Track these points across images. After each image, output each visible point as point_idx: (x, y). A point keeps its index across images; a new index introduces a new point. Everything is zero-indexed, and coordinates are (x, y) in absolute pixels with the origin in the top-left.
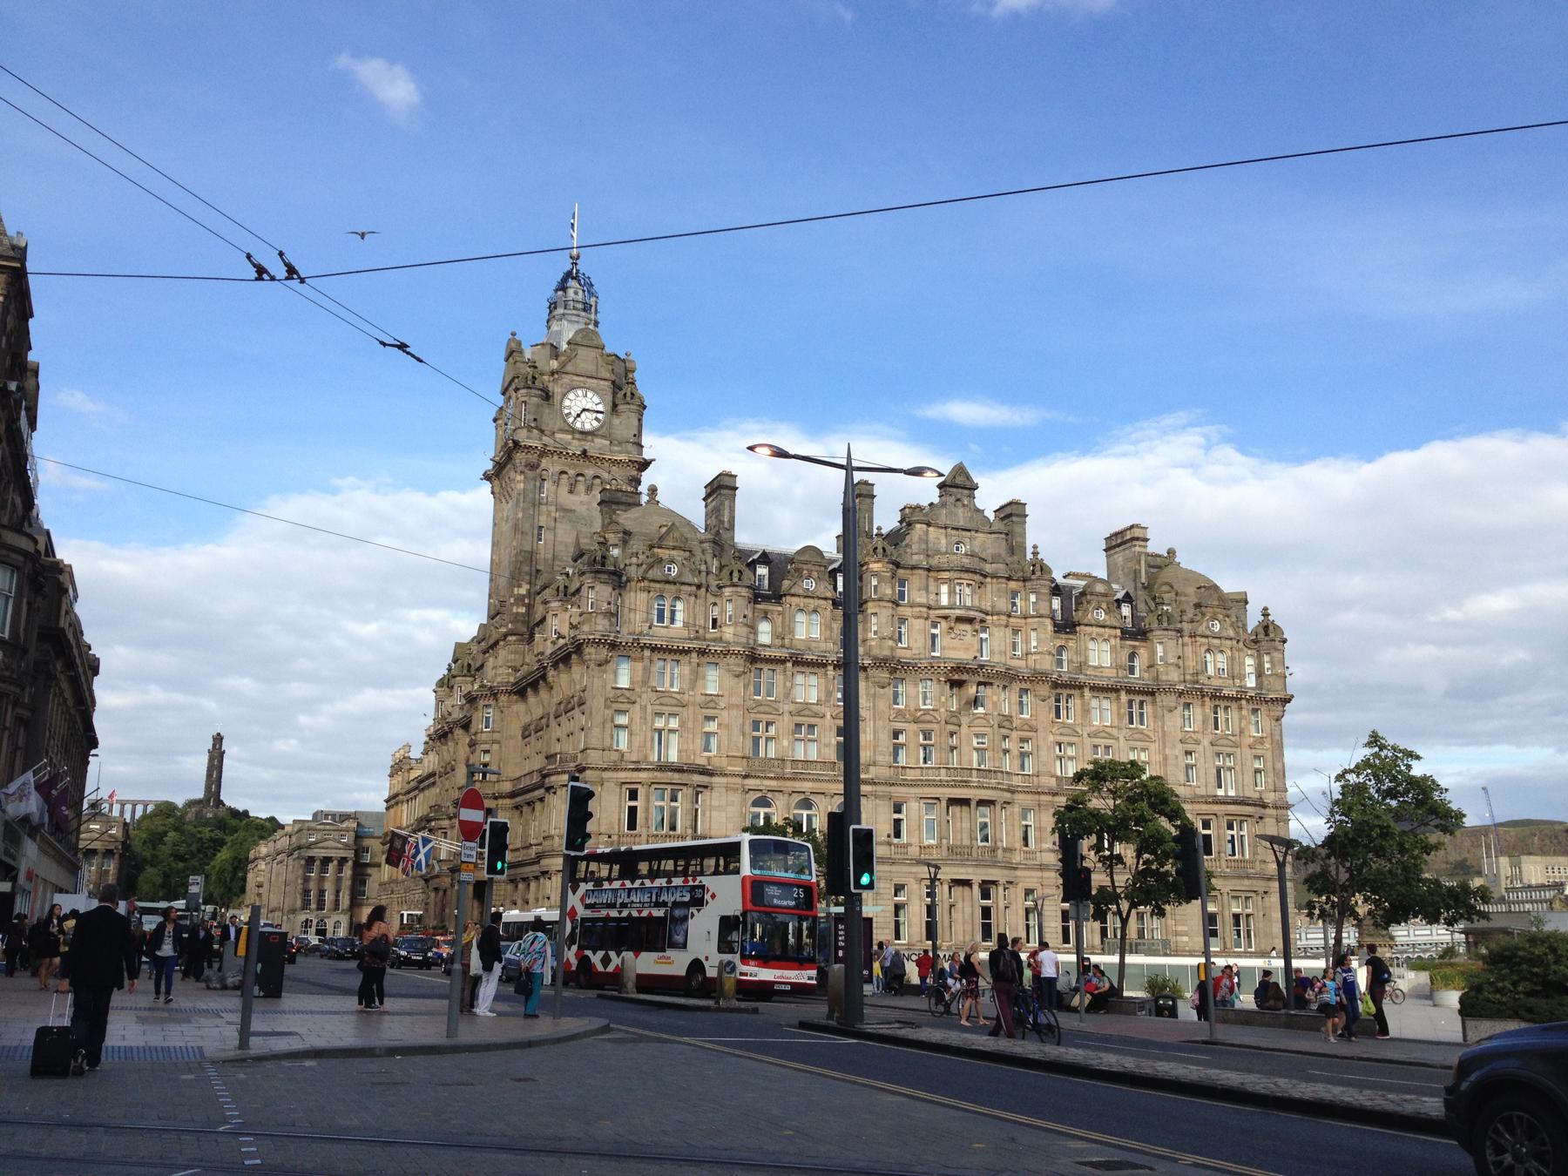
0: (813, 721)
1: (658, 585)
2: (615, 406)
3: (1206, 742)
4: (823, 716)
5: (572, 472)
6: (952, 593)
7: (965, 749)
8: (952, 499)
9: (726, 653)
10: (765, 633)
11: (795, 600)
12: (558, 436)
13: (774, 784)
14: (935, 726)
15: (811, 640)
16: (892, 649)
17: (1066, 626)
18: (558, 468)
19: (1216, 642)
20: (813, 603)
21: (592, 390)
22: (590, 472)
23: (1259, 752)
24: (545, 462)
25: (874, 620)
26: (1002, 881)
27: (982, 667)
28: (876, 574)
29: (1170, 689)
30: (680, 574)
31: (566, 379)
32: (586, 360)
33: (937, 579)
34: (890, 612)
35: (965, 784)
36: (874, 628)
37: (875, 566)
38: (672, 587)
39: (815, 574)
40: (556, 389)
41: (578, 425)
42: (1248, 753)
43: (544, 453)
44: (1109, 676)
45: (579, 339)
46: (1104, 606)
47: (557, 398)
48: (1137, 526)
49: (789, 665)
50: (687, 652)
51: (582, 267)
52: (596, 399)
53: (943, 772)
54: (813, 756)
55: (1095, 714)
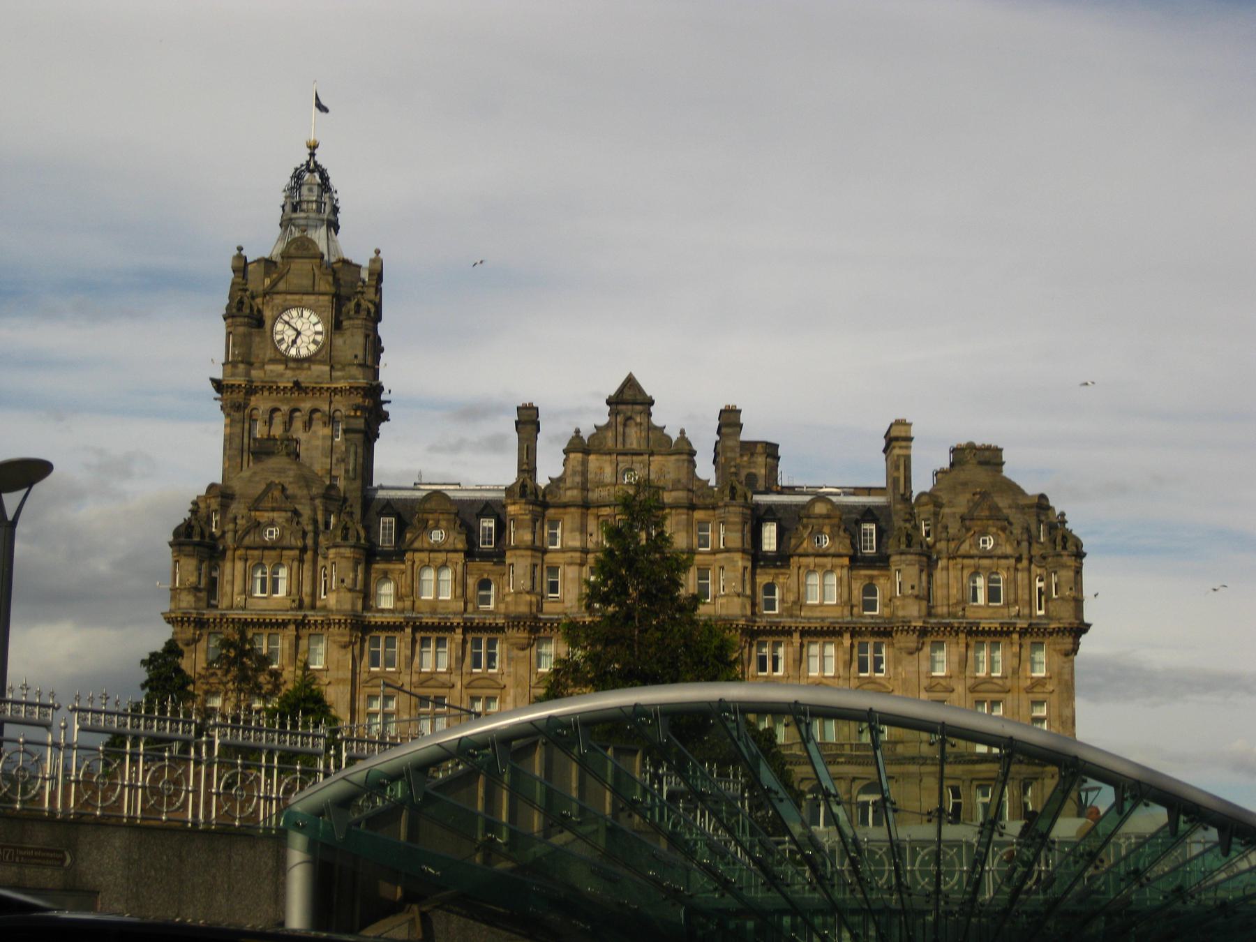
0: (440, 692)
1: (256, 553)
2: (336, 326)
3: (960, 689)
4: (453, 686)
5: (285, 408)
8: (620, 419)
9: (328, 624)
10: (386, 596)
11: (418, 556)
12: (269, 367)
18: (270, 405)
19: (985, 562)
20: (441, 557)
21: (310, 308)
22: (306, 406)
23: (1040, 697)
24: (254, 401)
29: (907, 629)
30: (282, 537)
31: (278, 299)
32: (300, 270)
34: (528, 561)
38: (273, 553)
39: (443, 523)
40: (268, 313)
41: (293, 352)
42: (1025, 699)
43: (251, 390)
45: (292, 251)
46: (827, 529)
47: (268, 323)
50: (284, 624)
51: (320, 158)
52: (314, 319)
55: (815, 664)
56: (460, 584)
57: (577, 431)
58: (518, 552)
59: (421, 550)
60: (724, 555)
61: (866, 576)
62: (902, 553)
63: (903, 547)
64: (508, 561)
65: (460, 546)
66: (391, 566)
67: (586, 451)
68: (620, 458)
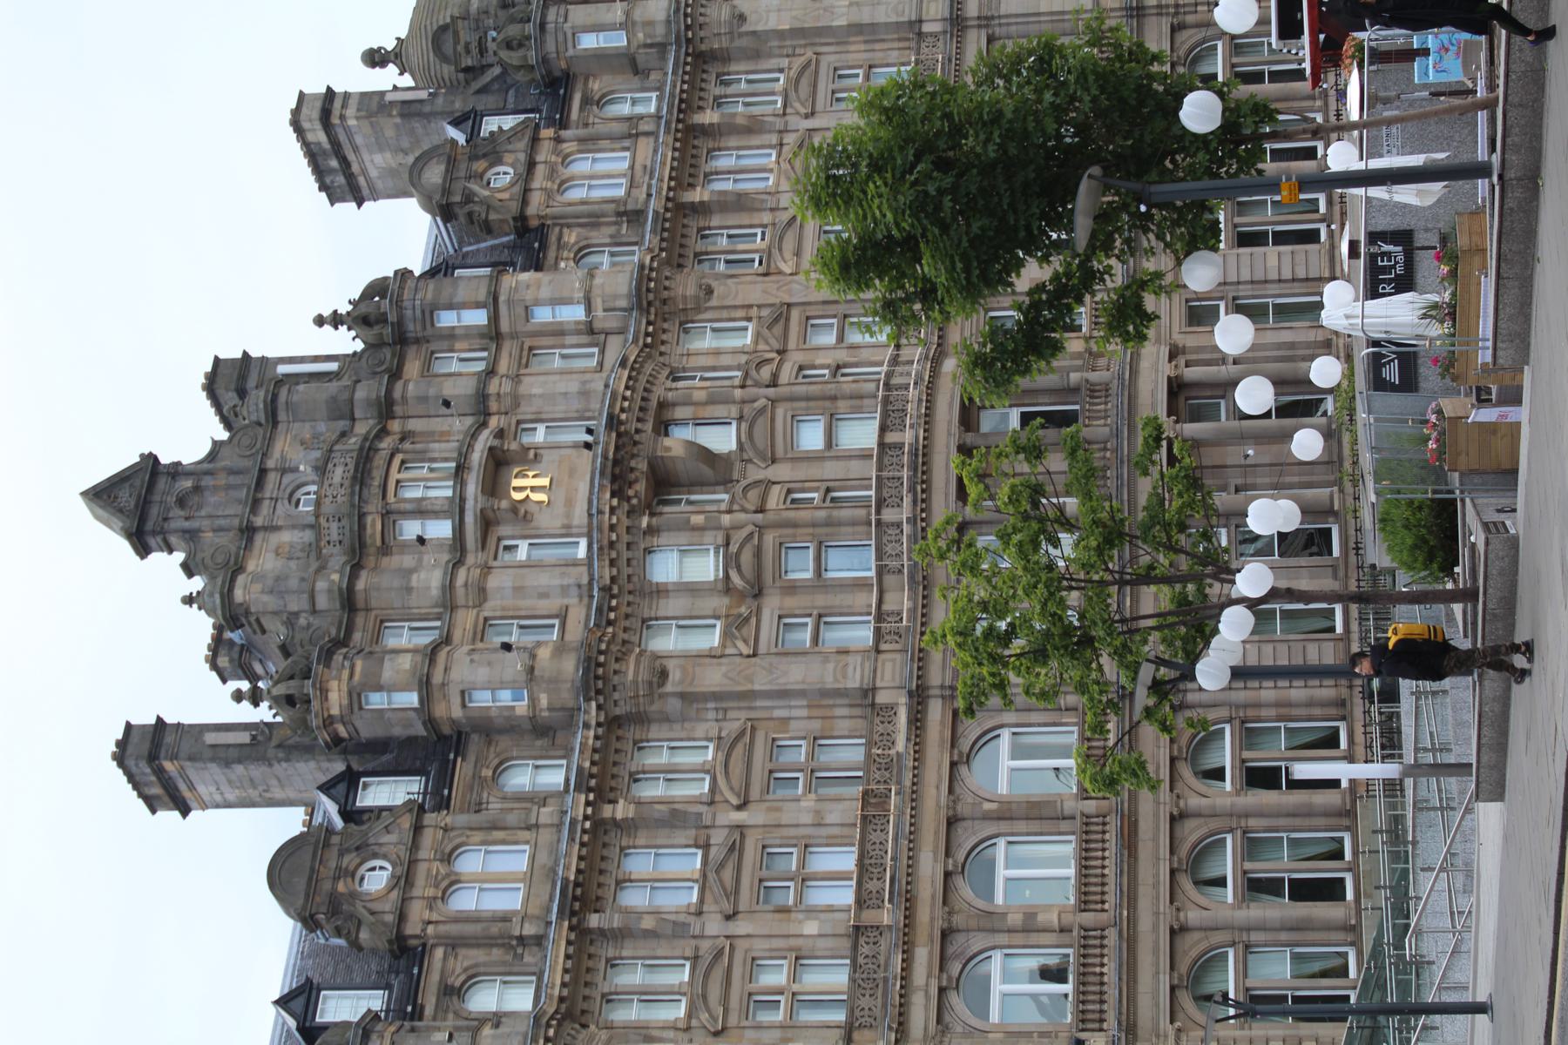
4: (741, 828)
6: (422, 511)
7: (831, 470)
11: (417, 912)
13: (922, 955)
14: (770, 538)
15: (529, 878)
16: (560, 648)
17: (530, 242)
25: (482, 699)
26: (1167, 370)
27: (613, 422)
28: (355, 698)
33: (385, 549)
35: (922, 457)
36: (505, 697)
37: (336, 700)
44: (657, 154)
46: (479, 166)
48: (296, 113)
49: (594, 921)
53: (889, 515)
54: (846, 860)
56: (494, 831)
57: (189, 600)
58: (437, 678)
59: (405, 900)
60: (503, 309)
61: (581, 109)
62: (542, 26)
63: (530, 28)
64: (457, 713)
65: (406, 822)
66: (435, 977)
67: (239, 569)
68: (265, 508)
